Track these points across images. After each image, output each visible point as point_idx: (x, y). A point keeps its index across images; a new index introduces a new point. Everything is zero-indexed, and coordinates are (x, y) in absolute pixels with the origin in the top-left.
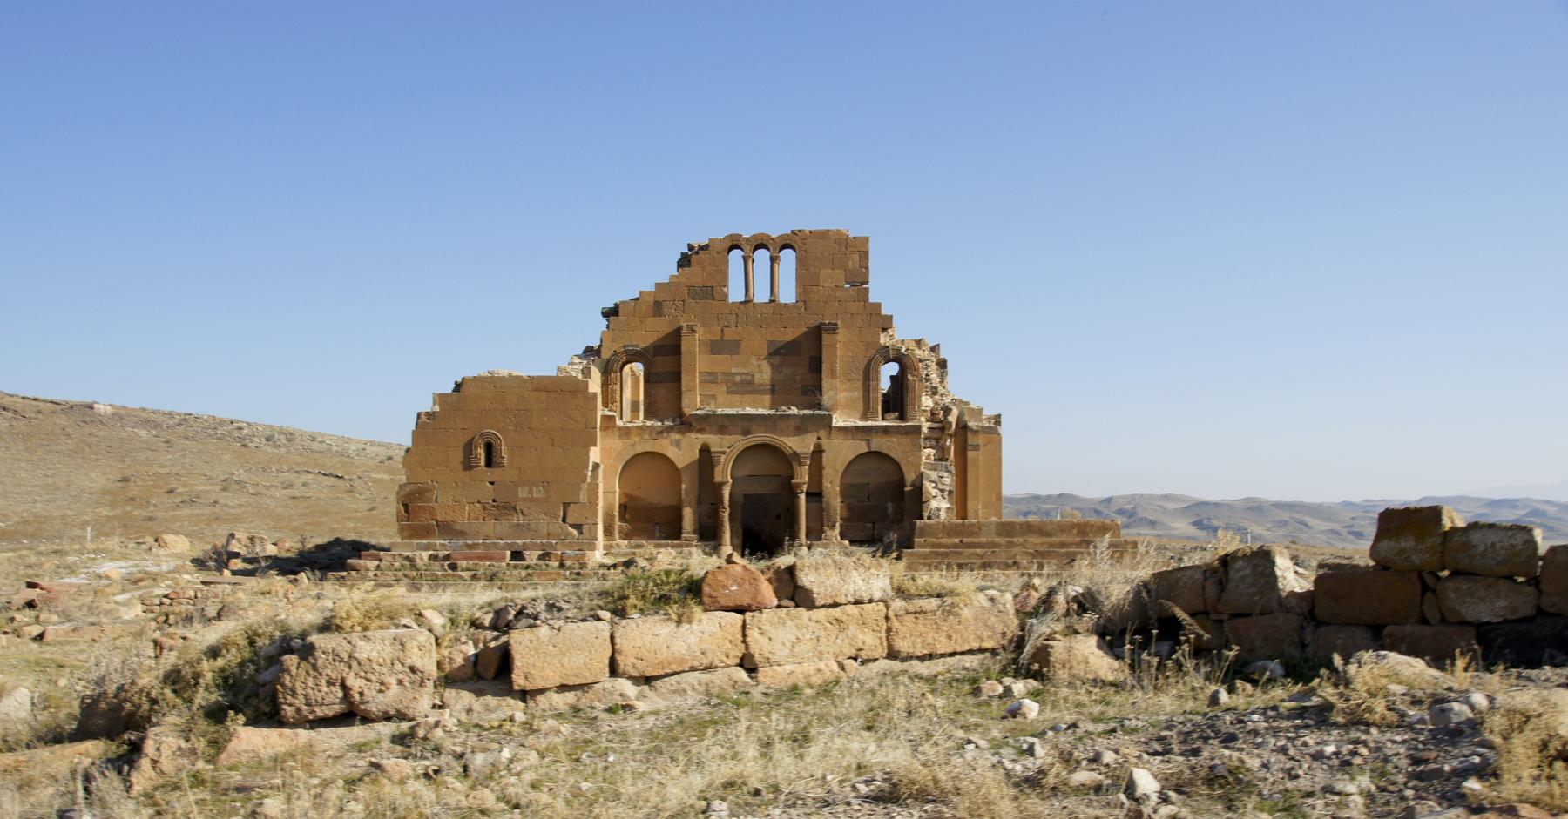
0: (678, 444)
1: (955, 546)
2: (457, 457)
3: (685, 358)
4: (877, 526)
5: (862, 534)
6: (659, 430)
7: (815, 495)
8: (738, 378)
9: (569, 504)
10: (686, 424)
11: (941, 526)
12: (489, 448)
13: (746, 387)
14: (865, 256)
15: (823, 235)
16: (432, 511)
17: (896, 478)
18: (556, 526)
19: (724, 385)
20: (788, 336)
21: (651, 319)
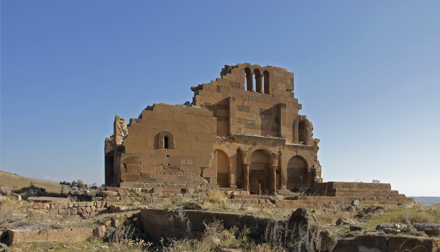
0: (229, 147)
1: (348, 192)
2: (151, 143)
3: (231, 111)
4: (297, 184)
5: (292, 188)
6: (222, 140)
7: (279, 172)
8: (249, 122)
9: (204, 168)
10: (232, 139)
11: (341, 184)
12: (166, 139)
13: (252, 126)
14: (292, 80)
15: (279, 69)
16: (138, 168)
17: (303, 167)
18: (198, 178)
19: (244, 124)
20: (268, 107)
21: (215, 93)
